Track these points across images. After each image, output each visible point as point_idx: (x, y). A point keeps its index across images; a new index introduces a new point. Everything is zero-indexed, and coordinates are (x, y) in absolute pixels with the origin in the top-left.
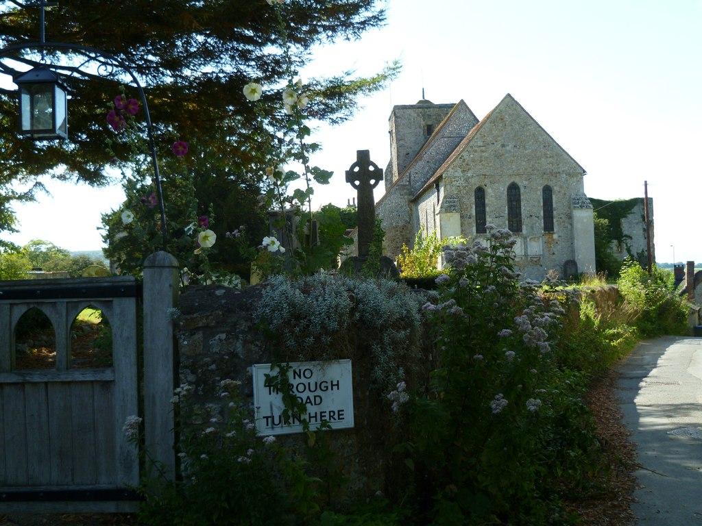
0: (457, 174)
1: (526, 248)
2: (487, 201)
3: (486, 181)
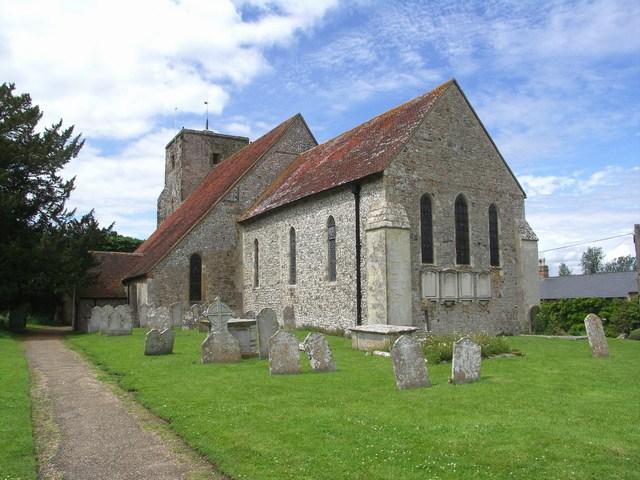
0: (400, 174)
1: (475, 287)
2: (434, 217)
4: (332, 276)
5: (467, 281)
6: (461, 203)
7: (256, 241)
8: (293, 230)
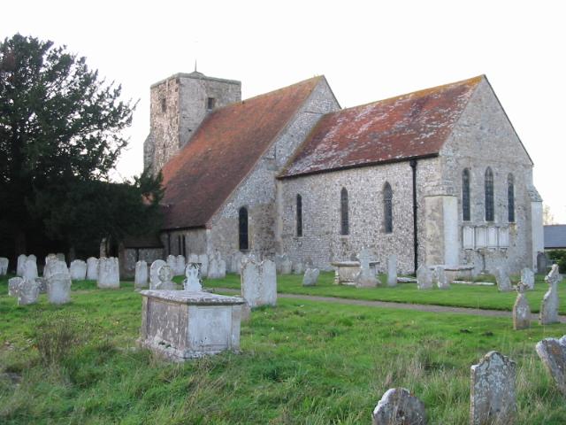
3: (471, 164)
4: (389, 229)
5: (492, 232)
6: (489, 174)
7: (299, 198)
8: (344, 192)
